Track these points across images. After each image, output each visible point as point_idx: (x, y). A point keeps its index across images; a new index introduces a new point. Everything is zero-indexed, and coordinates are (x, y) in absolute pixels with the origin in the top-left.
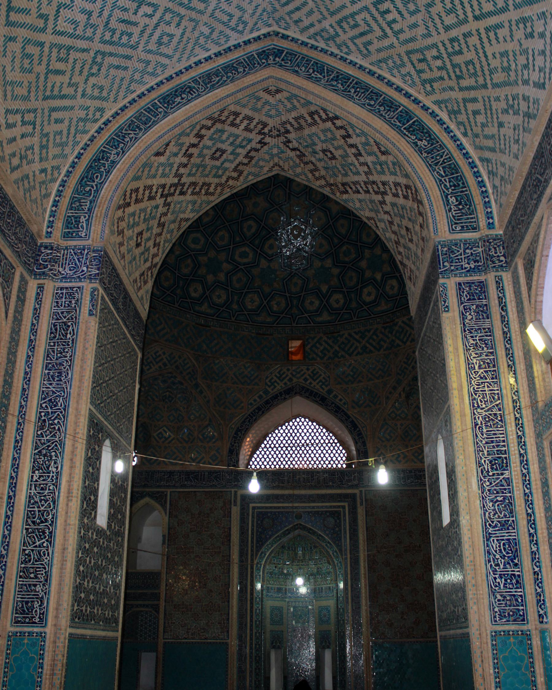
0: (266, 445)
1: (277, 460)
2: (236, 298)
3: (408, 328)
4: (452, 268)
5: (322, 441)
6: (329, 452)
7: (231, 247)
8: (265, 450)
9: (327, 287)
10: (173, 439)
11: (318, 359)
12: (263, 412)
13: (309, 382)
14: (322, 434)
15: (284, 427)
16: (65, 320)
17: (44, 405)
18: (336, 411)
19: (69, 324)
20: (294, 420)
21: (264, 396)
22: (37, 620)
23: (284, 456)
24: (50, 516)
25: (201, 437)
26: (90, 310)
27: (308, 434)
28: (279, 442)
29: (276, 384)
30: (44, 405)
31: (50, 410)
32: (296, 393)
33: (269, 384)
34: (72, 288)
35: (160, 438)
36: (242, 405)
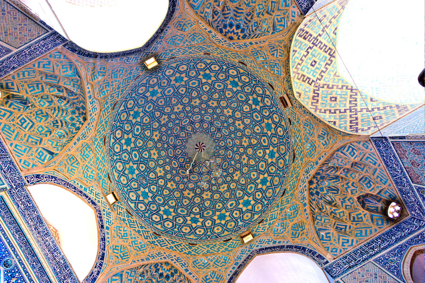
2: (118, 157)
3: (167, 242)
7: (137, 149)
9: (142, 199)
10: (24, 131)
11: (116, 212)
12: (75, 191)
13: (104, 213)
18: (102, 239)
21: (83, 189)
25: (39, 150)
29: (92, 193)
32: (95, 208)
33: (90, 190)
35: (20, 121)
36: (72, 176)
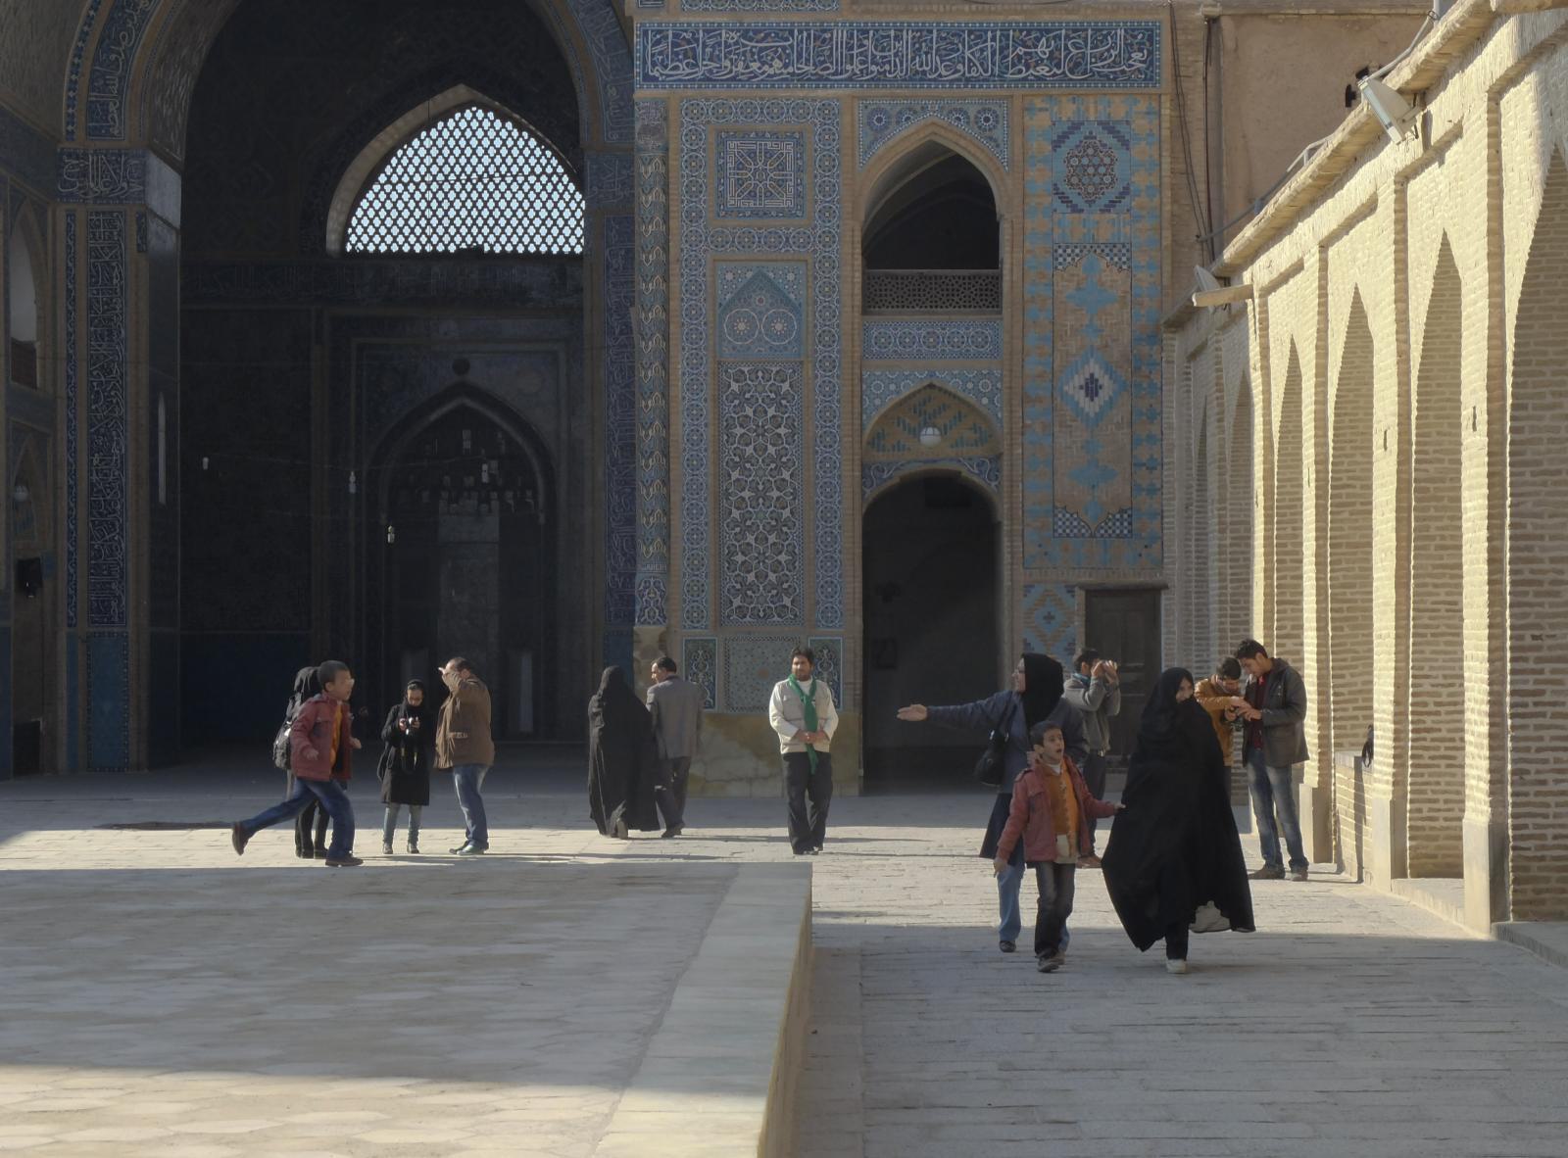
0: (389, 177)
1: (417, 213)
4: (601, 196)
5: (527, 170)
6: (544, 196)
8: (388, 188)
14: (527, 152)
15: (434, 133)
16: (107, 259)
17: (95, 373)
19: (114, 264)
20: (458, 115)
22: (116, 619)
23: (434, 205)
24: (119, 507)
26: (138, 245)
27: (492, 151)
28: (423, 169)
30: (95, 373)
31: (103, 379)
34: (111, 213)
